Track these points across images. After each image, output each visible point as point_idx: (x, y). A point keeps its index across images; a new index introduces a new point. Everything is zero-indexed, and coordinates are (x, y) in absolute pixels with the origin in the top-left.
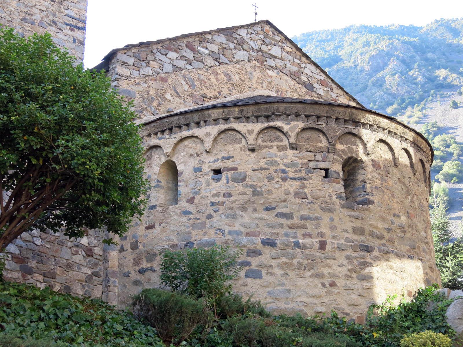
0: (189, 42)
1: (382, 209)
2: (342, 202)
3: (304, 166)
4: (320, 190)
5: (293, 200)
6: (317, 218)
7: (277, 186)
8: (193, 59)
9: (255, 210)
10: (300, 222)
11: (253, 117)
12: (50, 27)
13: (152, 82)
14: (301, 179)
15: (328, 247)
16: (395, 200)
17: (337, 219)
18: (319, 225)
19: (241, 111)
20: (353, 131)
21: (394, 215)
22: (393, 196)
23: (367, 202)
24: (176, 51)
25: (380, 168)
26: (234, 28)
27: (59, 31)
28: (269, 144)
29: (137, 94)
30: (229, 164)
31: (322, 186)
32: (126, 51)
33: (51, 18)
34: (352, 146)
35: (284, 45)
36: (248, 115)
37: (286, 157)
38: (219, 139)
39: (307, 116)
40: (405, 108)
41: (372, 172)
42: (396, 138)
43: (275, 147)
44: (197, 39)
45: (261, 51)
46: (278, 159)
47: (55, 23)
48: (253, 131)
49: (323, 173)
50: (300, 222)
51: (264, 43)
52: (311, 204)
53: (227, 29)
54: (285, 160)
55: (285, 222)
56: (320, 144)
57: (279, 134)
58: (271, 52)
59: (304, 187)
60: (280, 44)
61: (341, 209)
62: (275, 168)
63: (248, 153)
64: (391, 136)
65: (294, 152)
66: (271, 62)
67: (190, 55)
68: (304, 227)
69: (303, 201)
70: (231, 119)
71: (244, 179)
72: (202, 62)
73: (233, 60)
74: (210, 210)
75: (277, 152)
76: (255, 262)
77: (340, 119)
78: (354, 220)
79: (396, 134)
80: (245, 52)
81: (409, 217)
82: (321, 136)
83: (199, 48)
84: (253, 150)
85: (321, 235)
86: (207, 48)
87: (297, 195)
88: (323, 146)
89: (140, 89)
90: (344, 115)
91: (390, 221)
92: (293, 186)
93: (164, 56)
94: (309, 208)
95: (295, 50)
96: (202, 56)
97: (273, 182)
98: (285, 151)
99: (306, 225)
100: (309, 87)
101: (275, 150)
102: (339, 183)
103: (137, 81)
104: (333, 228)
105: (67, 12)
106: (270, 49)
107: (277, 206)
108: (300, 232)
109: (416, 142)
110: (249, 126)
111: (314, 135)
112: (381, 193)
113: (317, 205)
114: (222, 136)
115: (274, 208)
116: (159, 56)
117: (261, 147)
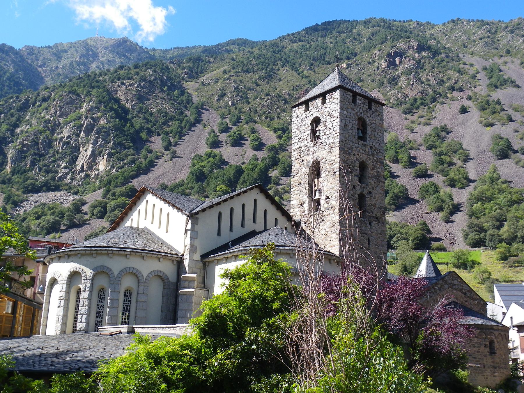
15: (486, 367)
23: (495, 353)
40: (418, 108)
51: (453, 280)
55: (473, 359)
66: (455, 287)
67: (433, 290)
68: (479, 361)
85: (484, 364)
87: (478, 352)
100: (465, 294)
104: (487, 362)
108: (478, 363)
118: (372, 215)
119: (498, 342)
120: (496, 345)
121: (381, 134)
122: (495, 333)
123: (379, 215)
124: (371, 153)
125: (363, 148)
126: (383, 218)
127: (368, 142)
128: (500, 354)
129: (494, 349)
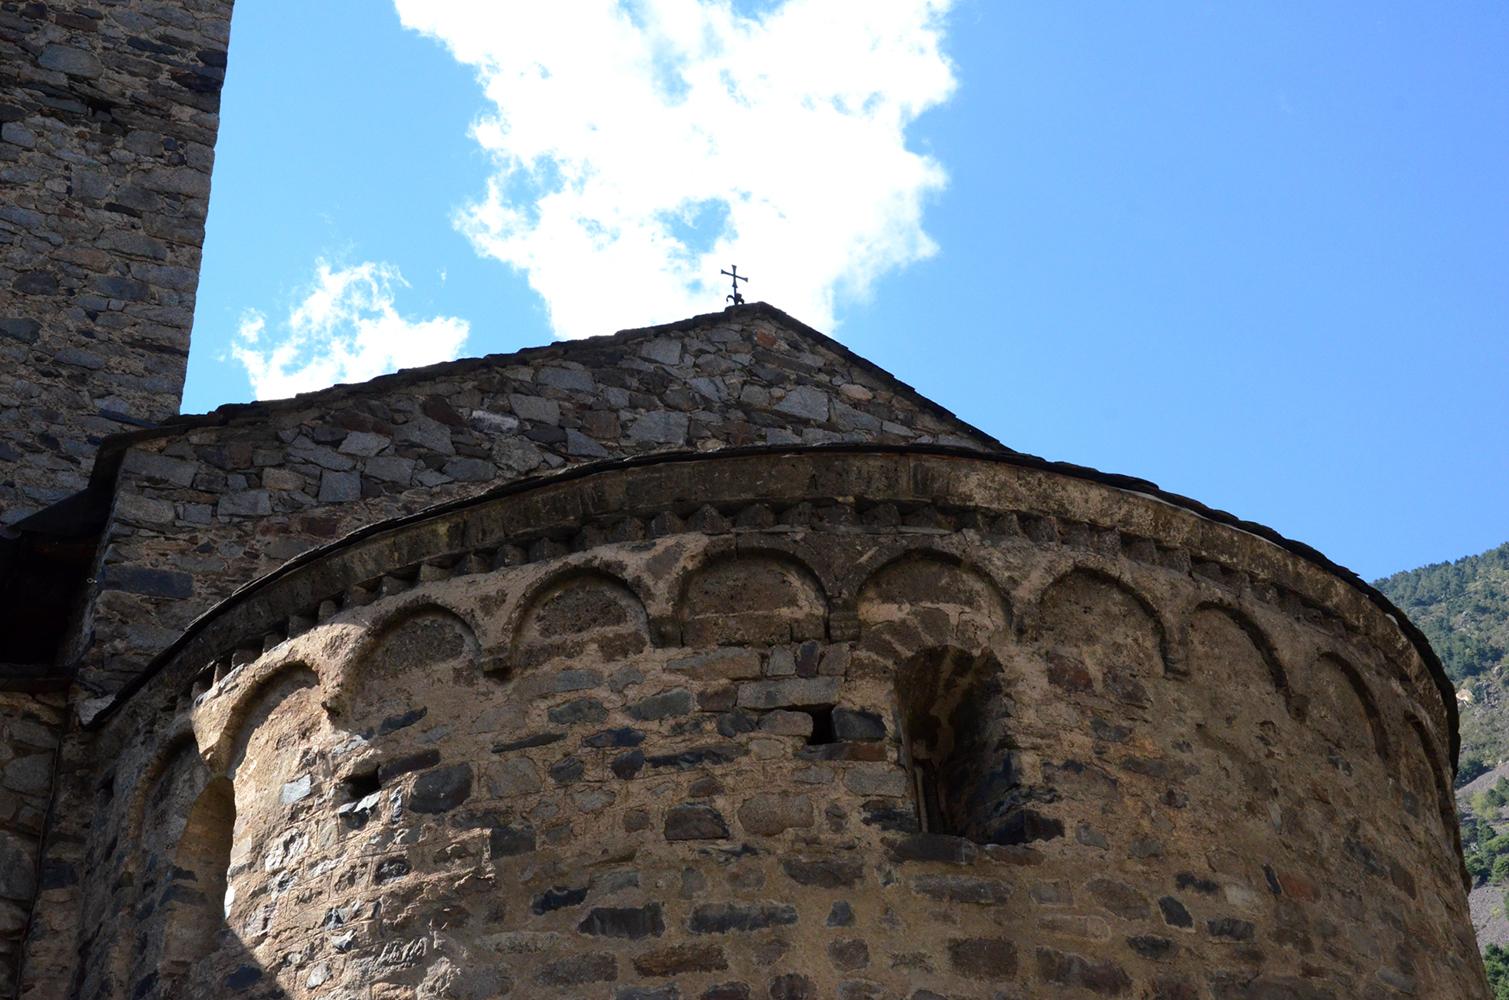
0: (435, 398)
1: (1110, 856)
2: (891, 835)
3: (714, 706)
4: (785, 794)
5: (661, 850)
6: (770, 918)
7: (597, 800)
8: (451, 449)
9: (497, 916)
10: (689, 942)
11: (508, 548)
12: (28, 457)
13: (268, 538)
14: (696, 757)
16: (1183, 818)
17: (866, 914)
18: (781, 945)
19: (459, 533)
20: (939, 544)
21: (1184, 880)
22: (1170, 799)
23: (1025, 829)
24: (378, 430)
25: (1089, 683)
26: (625, 337)
27: (65, 464)
28: (571, 637)
29: (196, 585)
31: (799, 775)
32: (163, 443)
33: (38, 425)
34: (942, 606)
35: (837, 381)
36: (489, 542)
37: (634, 677)
38: (379, 654)
39: (730, 511)
41: (1046, 701)
42: (1172, 566)
43: (595, 646)
44: (469, 385)
45: (746, 408)
46: (601, 693)
47: (50, 441)
48: (501, 598)
49: (806, 725)
50: (695, 940)
51: (751, 375)
52: (746, 859)
53: (596, 343)
54: (632, 693)
55: (622, 949)
56: (785, 612)
57: (610, 594)
58: (784, 407)
59: (711, 788)
60: (824, 378)
61: (888, 867)
62: (590, 729)
63: (483, 684)
64: (1138, 557)
65: (673, 652)
67: (439, 438)
68: (708, 960)
69: (709, 847)
70: (425, 570)
71: (461, 793)
72: (487, 456)
73: (624, 443)
75: (600, 666)
77: (875, 504)
78: (958, 910)
79: (1164, 550)
80: (674, 416)
81: (1275, 890)
82: (795, 580)
83: (476, 414)
84: (500, 673)
86: (510, 412)
87: (678, 826)
88: (799, 615)
89: (213, 563)
90: (889, 487)
91: (1155, 908)
92: (658, 793)
93: (328, 449)
94: (734, 878)
95: (884, 395)
96: (492, 440)
97: (578, 786)
98: (632, 657)
99: (720, 952)
101: (590, 659)
102: (881, 756)
103: (203, 539)
104: (849, 954)
105: (101, 404)
106: (780, 399)
107: (592, 883)
109: (1288, 582)
110: (489, 583)
111: (765, 576)
112: (1105, 789)
113: (772, 859)
114: (391, 640)
115: (577, 897)
116: (303, 449)
117: (534, 657)
118: (28, 71)
119: (1067, 679)
120: (1036, 713)
122: (997, 560)
123: (119, 84)
126: (184, 114)
128: (1150, 851)
129: (1009, 775)
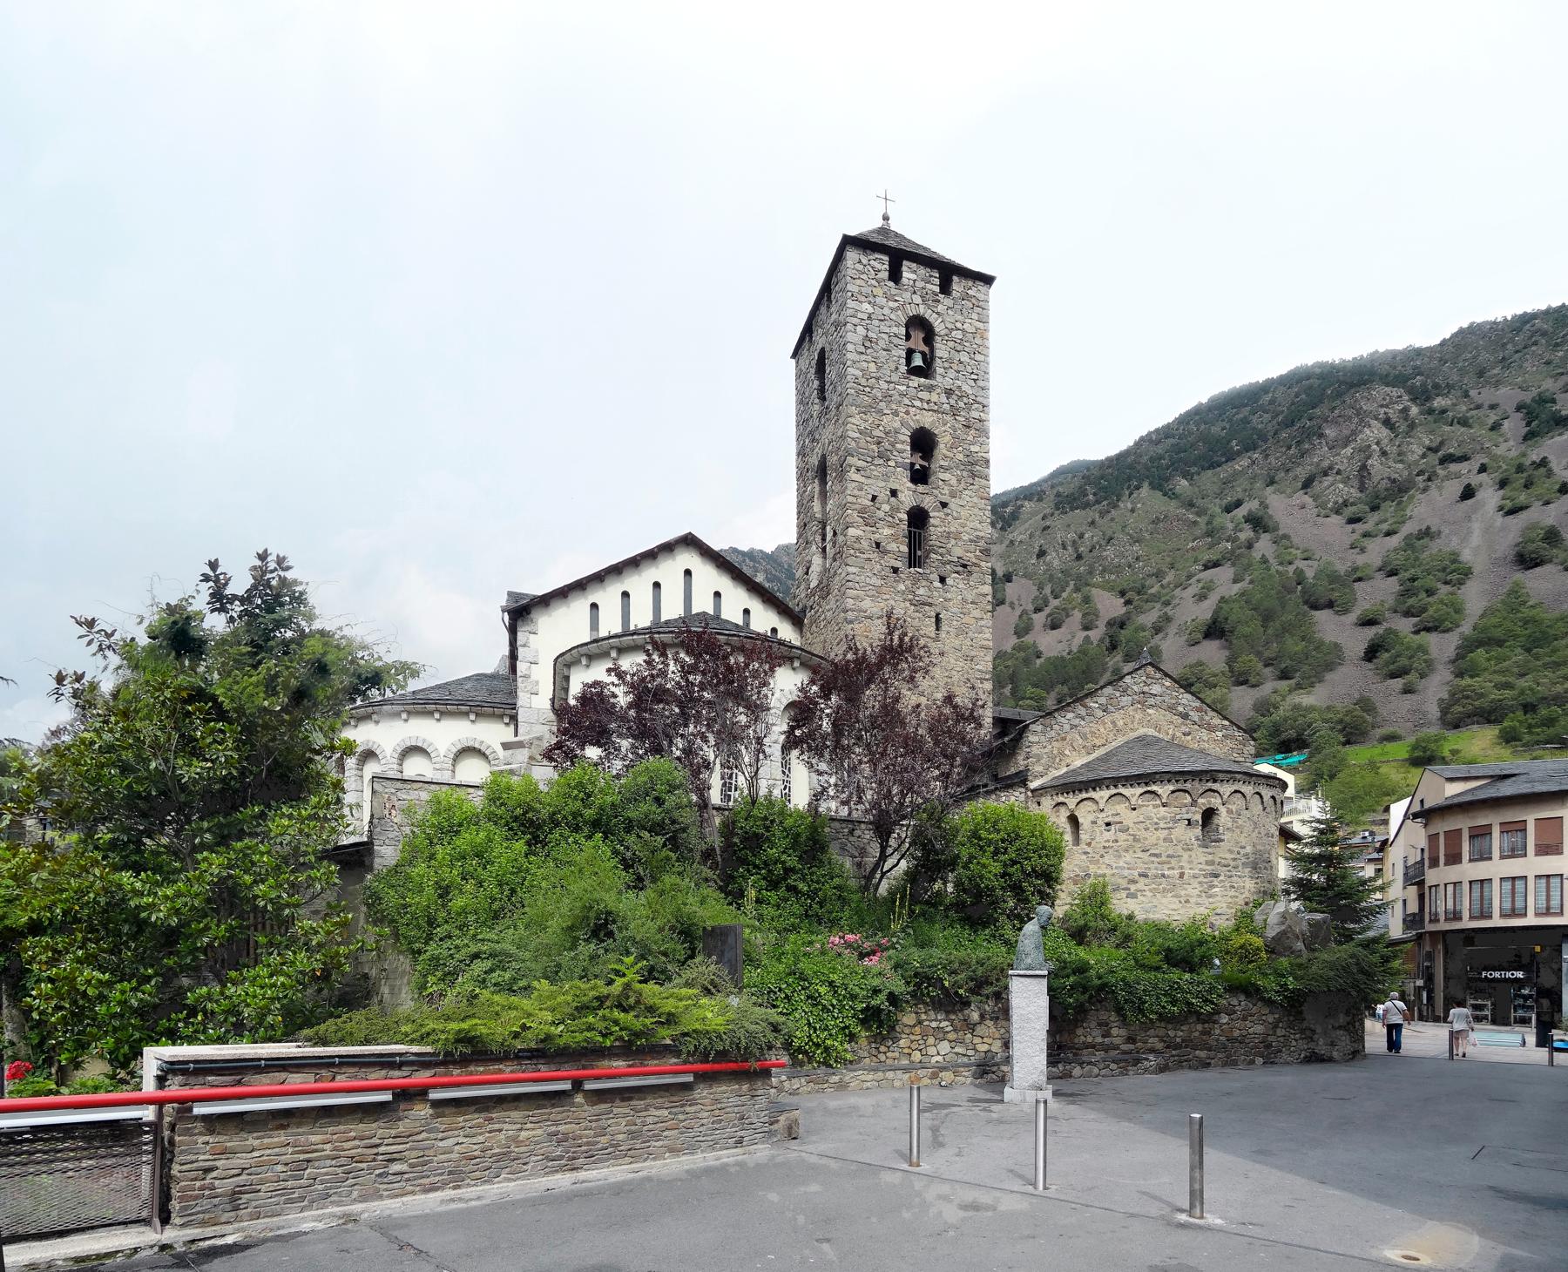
30: (1117, 819)
74: (1102, 852)
76: (1133, 888)
92: (1163, 834)
119: (1229, 811)
120: (1223, 819)
121: (978, 357)
124: (946, 407)
125: (924, 395)
127: (939, 378)
